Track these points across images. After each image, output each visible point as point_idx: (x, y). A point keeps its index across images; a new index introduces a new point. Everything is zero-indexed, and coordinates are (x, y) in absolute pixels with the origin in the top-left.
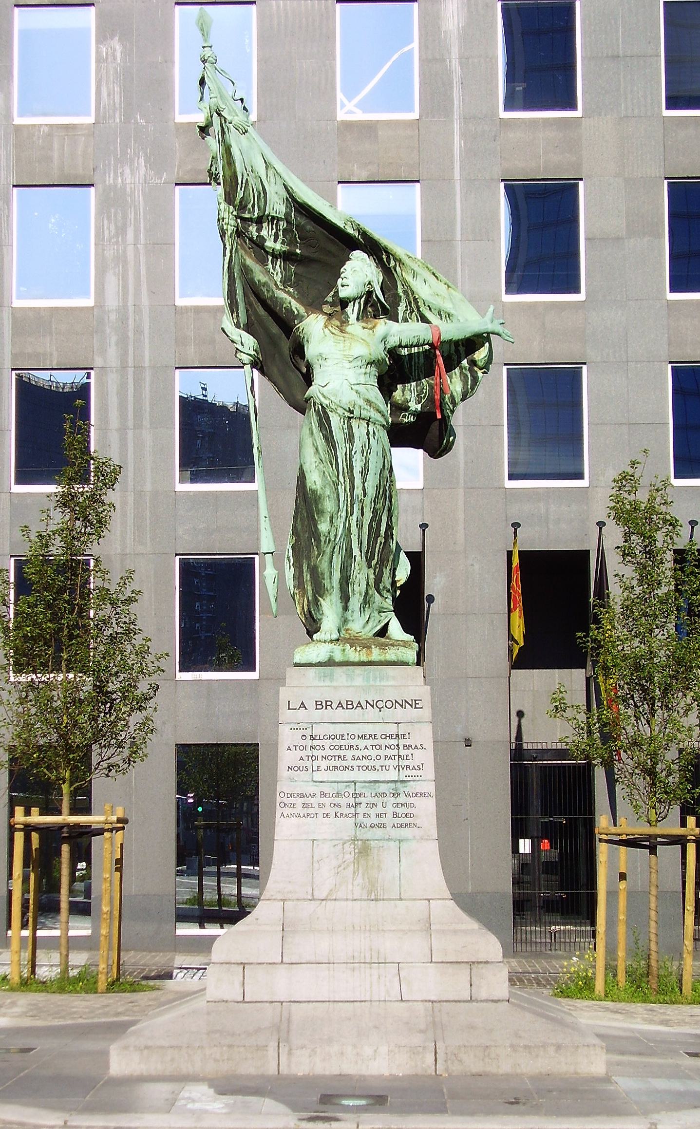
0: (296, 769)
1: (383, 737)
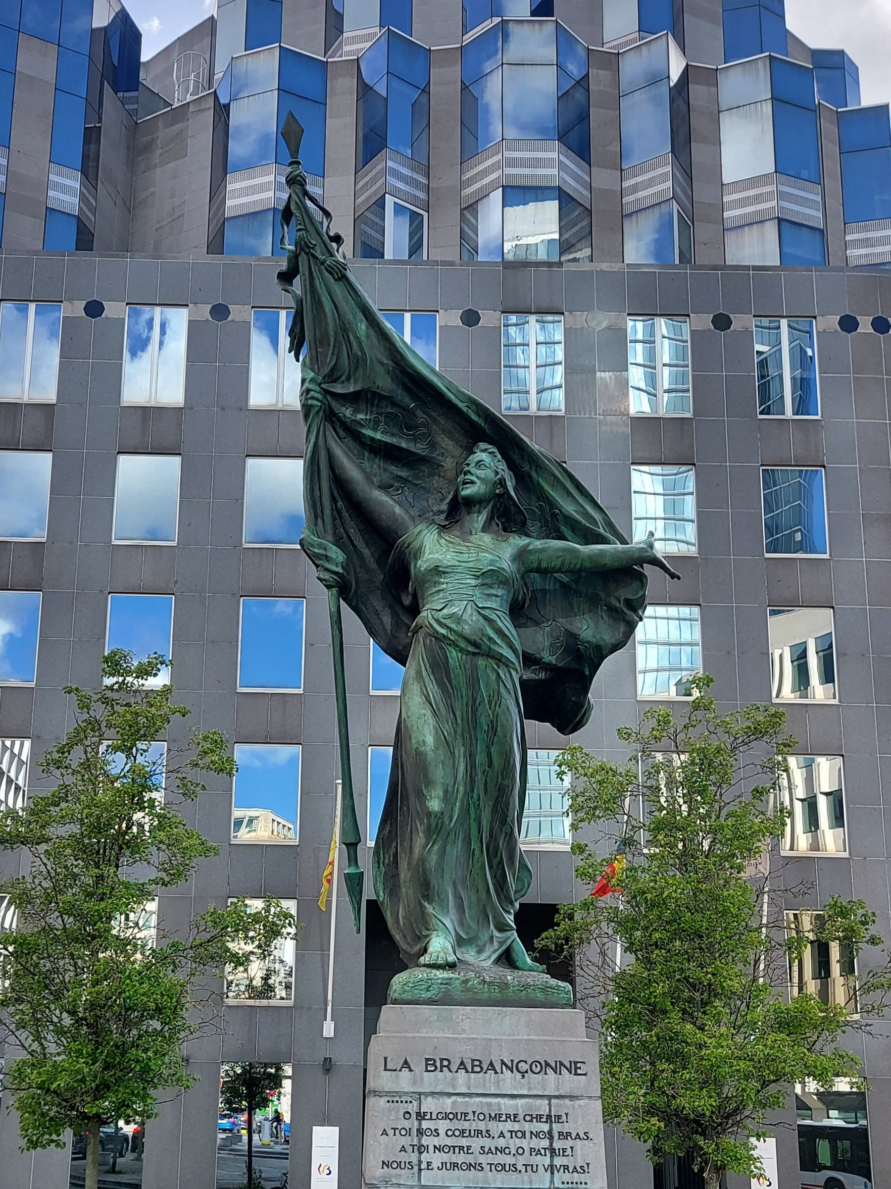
0: (395, 1165)
1: (528, 1118)
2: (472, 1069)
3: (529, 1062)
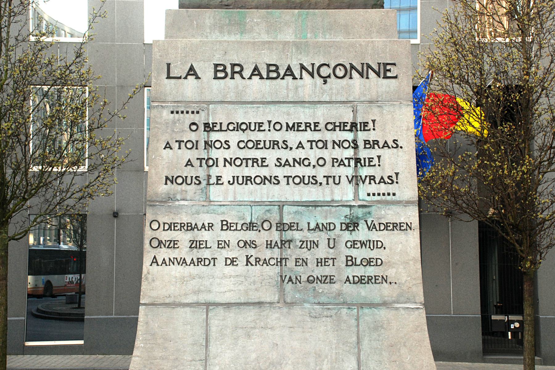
0: (180, 180)
1: (330, 127)
2: (268, 75)
3: (332, 65)
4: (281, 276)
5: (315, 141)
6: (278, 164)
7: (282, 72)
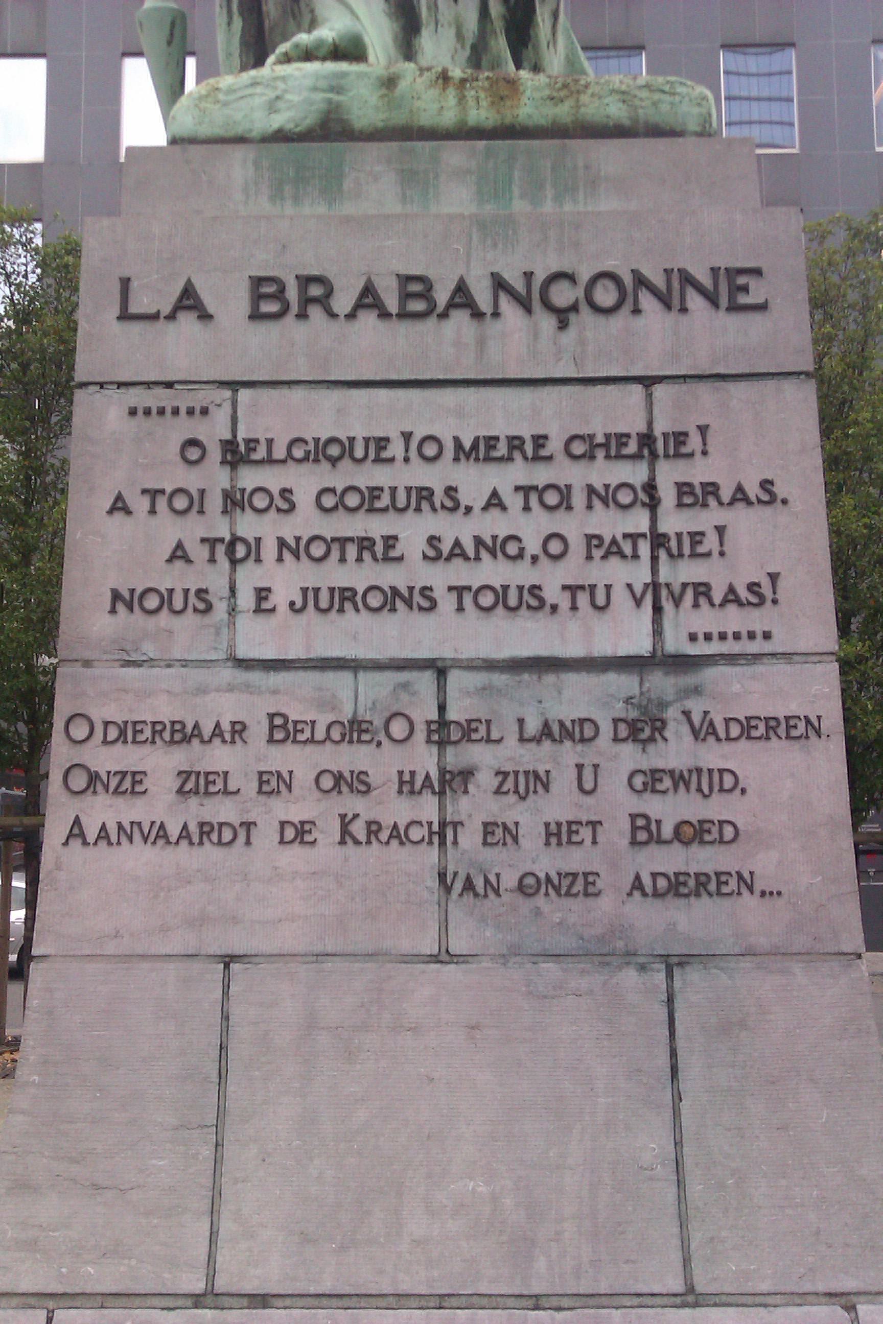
1: (578, 448)
3: (584, 276)
4: (442, 876)
5: (535, 488)
6: (431, 553)
7: (442, 297)
